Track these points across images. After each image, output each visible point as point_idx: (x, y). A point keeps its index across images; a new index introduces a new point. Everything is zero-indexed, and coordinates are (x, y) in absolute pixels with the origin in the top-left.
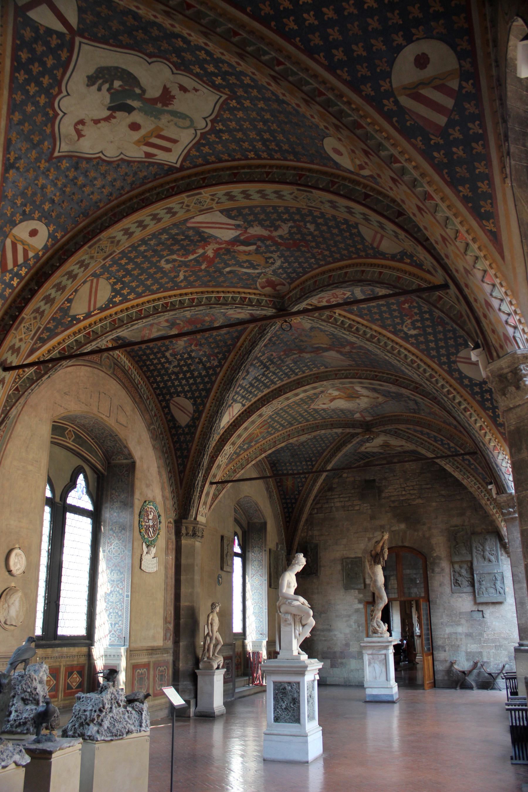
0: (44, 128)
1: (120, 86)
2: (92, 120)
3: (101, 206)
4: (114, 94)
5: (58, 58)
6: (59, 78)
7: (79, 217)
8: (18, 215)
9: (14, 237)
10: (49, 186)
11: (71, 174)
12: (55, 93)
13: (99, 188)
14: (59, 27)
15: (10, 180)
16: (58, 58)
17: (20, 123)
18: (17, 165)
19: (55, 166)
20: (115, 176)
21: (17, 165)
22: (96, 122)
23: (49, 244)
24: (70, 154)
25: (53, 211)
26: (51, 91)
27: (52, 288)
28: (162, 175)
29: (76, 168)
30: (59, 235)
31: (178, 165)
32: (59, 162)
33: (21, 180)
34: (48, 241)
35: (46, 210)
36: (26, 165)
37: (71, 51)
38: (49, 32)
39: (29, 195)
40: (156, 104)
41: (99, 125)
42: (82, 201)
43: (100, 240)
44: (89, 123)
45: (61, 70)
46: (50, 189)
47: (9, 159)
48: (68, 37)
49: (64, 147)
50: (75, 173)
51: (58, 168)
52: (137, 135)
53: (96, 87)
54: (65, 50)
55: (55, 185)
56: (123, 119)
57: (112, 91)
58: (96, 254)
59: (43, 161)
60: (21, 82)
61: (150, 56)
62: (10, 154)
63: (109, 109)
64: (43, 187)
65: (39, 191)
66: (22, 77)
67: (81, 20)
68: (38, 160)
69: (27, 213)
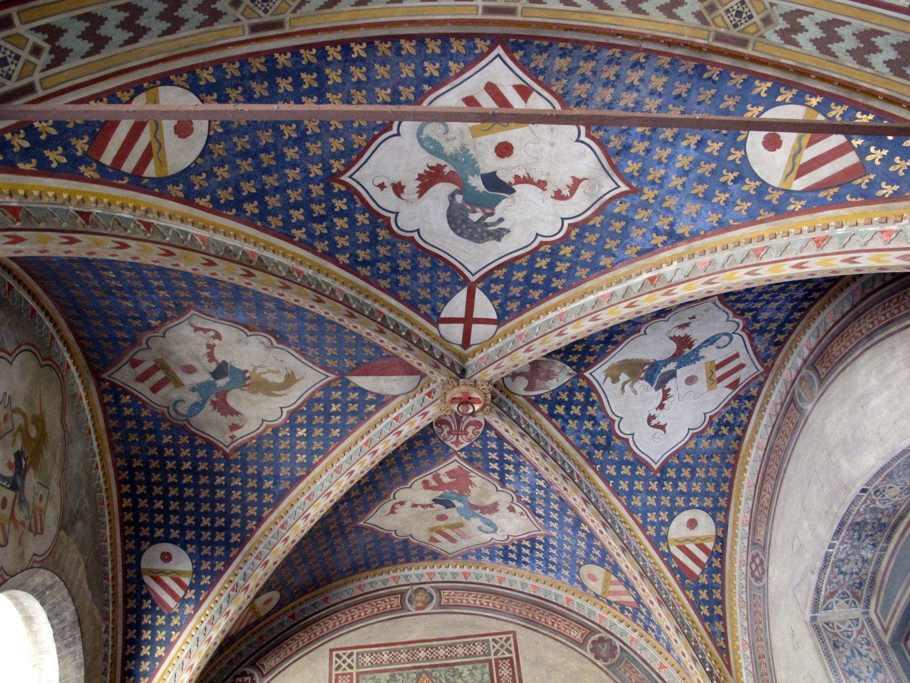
1: (474, 212)
2: (544, 189)
3: (668, 59)
4: (489, 205)
5: (509, 274)
6: (528, 257)
8: (745, 188)
9: (787, 176)
10: (678, 165)
12: (549, 246)
13: (638, 91)
14: (480, 296)
15: (692, 227)
16: (509, 274)
17: (609, 253)
18: (667, 228)
19: (641, 178)
20: (600, 90)
21: (667, 228)
22: (542, 185)
23: (789, 95)
24: (611, 172)
27: (869, 65)
28: (537, 42)
29: (627, 147)
30: (762, 88)
31: (499, 50)
32: (633, 176)
33: (685, 212)
34: (783, 103)
35: (721, 144)
36: (661, 217)
37: (491, 272)
38: (492, 297)
39: (706, 186)
40: (451, 172)
41: (543, 178)
42: (678, 97)
43: (719, 37)
44: (551, 189)
45: (517, 263)
48: (482, 284)
49: (608, 186)
50: (635, 143)
51: (643, 172)
53: (501, 226)
54: (494, 276)
55: (671, 157)
56: (506, 169)
57: (488, 211)
58: (757, 18)
59: (644, 198)
60: (564, 281)
61: (412, 239)
62: (656, 245)
63: (513, 191)
64: (683, 173)
65: (692, 176)
66: (557, 283)
67: (453, 294)
68: (645, 205)
69: (736, 174)
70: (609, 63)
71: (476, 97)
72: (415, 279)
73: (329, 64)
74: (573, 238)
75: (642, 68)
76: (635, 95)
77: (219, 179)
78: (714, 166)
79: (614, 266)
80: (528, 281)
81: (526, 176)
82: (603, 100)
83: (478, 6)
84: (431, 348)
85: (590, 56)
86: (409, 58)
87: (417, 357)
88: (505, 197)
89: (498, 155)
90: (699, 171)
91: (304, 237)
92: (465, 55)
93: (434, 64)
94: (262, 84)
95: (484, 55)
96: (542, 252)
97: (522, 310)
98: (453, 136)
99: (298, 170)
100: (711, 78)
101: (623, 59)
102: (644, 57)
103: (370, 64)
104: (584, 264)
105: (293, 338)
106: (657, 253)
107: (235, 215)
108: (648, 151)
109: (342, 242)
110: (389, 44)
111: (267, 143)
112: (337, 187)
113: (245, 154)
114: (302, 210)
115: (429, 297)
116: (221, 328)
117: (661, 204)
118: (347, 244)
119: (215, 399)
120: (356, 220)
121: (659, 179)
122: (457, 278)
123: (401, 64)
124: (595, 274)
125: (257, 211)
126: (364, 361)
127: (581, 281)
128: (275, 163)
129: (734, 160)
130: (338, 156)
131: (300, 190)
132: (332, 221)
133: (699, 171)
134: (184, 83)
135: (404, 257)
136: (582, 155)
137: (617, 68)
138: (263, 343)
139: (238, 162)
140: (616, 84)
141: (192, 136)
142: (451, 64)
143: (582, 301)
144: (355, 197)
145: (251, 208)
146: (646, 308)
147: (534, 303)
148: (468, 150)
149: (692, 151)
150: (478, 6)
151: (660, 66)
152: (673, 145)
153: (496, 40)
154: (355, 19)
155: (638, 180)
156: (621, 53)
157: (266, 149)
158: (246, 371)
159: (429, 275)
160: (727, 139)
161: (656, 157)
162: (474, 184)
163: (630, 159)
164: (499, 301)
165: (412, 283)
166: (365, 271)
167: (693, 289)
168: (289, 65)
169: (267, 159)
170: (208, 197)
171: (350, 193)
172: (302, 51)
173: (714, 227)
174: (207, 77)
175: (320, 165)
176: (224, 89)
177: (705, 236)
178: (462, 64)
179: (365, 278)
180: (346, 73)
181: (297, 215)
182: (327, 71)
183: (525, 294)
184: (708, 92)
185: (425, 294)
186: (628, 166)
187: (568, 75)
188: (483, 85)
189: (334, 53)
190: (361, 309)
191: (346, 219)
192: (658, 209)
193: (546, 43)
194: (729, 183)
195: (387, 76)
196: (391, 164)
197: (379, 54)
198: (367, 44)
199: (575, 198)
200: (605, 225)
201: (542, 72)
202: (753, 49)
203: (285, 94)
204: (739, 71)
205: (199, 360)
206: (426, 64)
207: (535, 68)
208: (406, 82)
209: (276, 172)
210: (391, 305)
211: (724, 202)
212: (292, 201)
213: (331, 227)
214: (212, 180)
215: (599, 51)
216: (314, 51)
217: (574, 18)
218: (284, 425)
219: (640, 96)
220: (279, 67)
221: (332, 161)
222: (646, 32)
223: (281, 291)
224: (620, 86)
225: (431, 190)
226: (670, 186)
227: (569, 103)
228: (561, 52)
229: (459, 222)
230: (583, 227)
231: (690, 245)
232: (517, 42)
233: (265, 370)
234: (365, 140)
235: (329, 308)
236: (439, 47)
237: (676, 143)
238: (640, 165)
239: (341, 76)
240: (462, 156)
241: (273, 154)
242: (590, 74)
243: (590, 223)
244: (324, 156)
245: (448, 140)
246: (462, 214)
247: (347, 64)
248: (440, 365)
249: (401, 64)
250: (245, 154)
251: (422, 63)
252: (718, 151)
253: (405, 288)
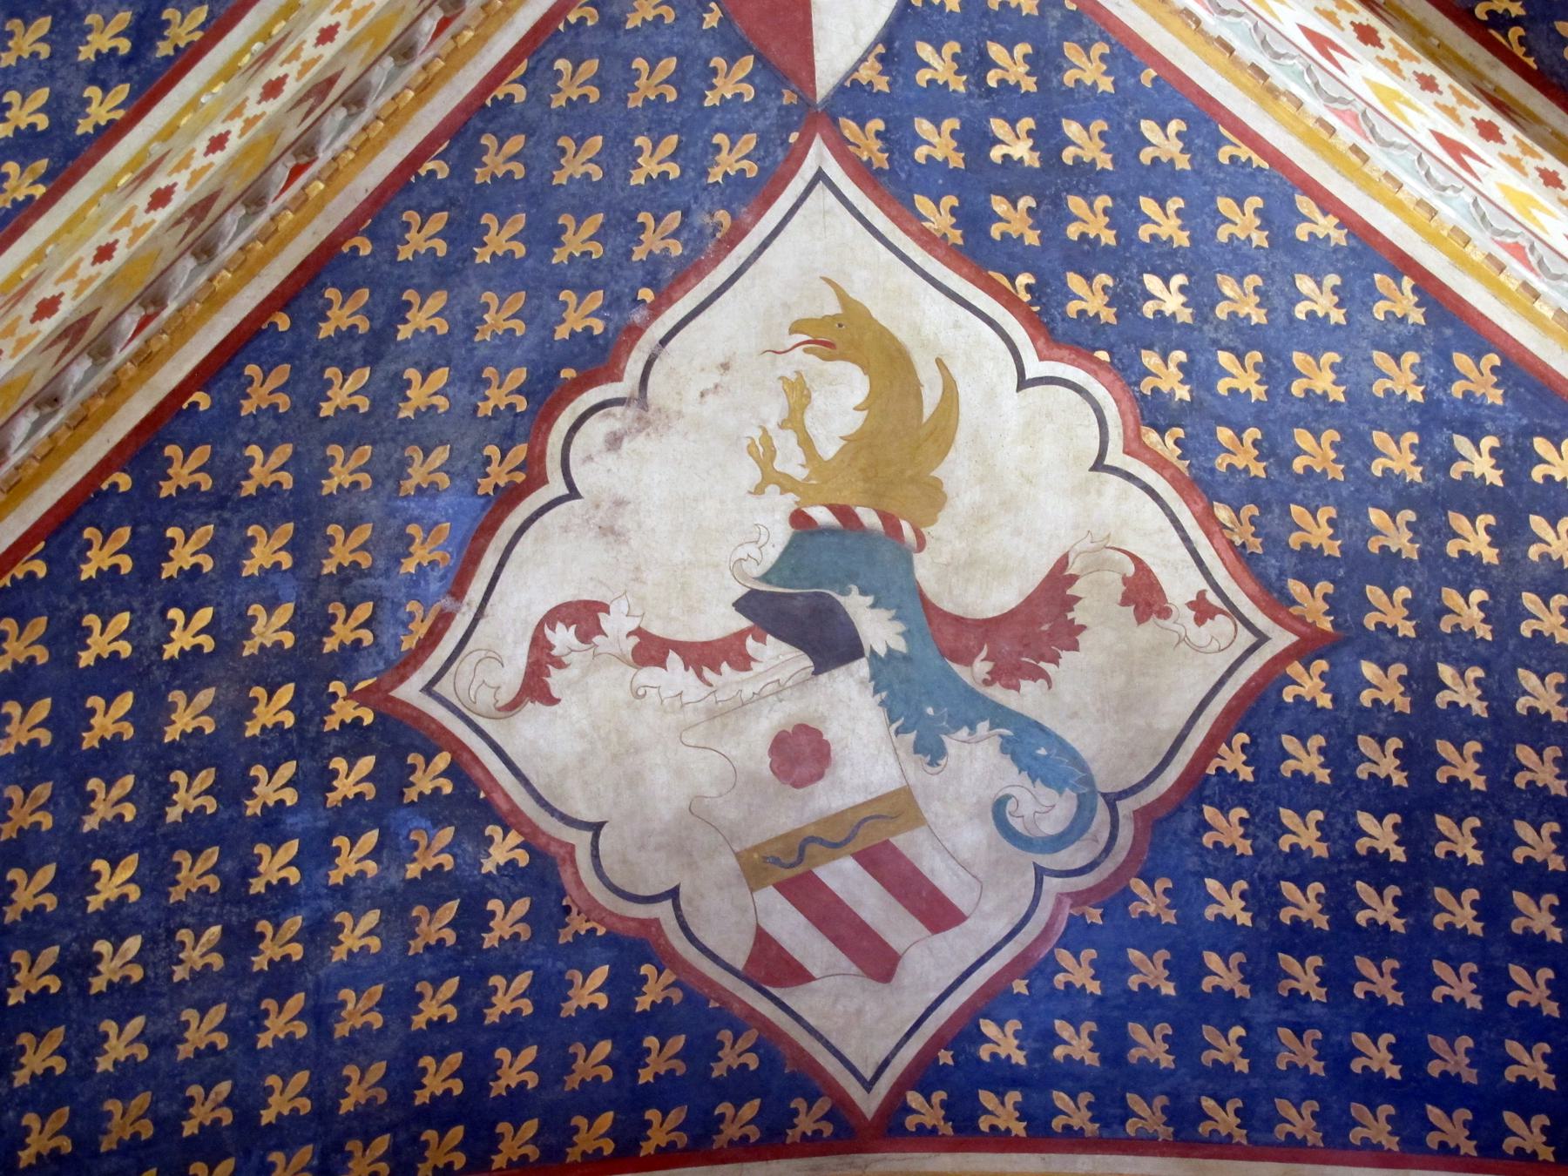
105: (580, 315)
118: (42, 95)
119: (982, 667)
138: (614, 442)
158: (799, 519)
205: (742, 706)
218: (1126, 373)
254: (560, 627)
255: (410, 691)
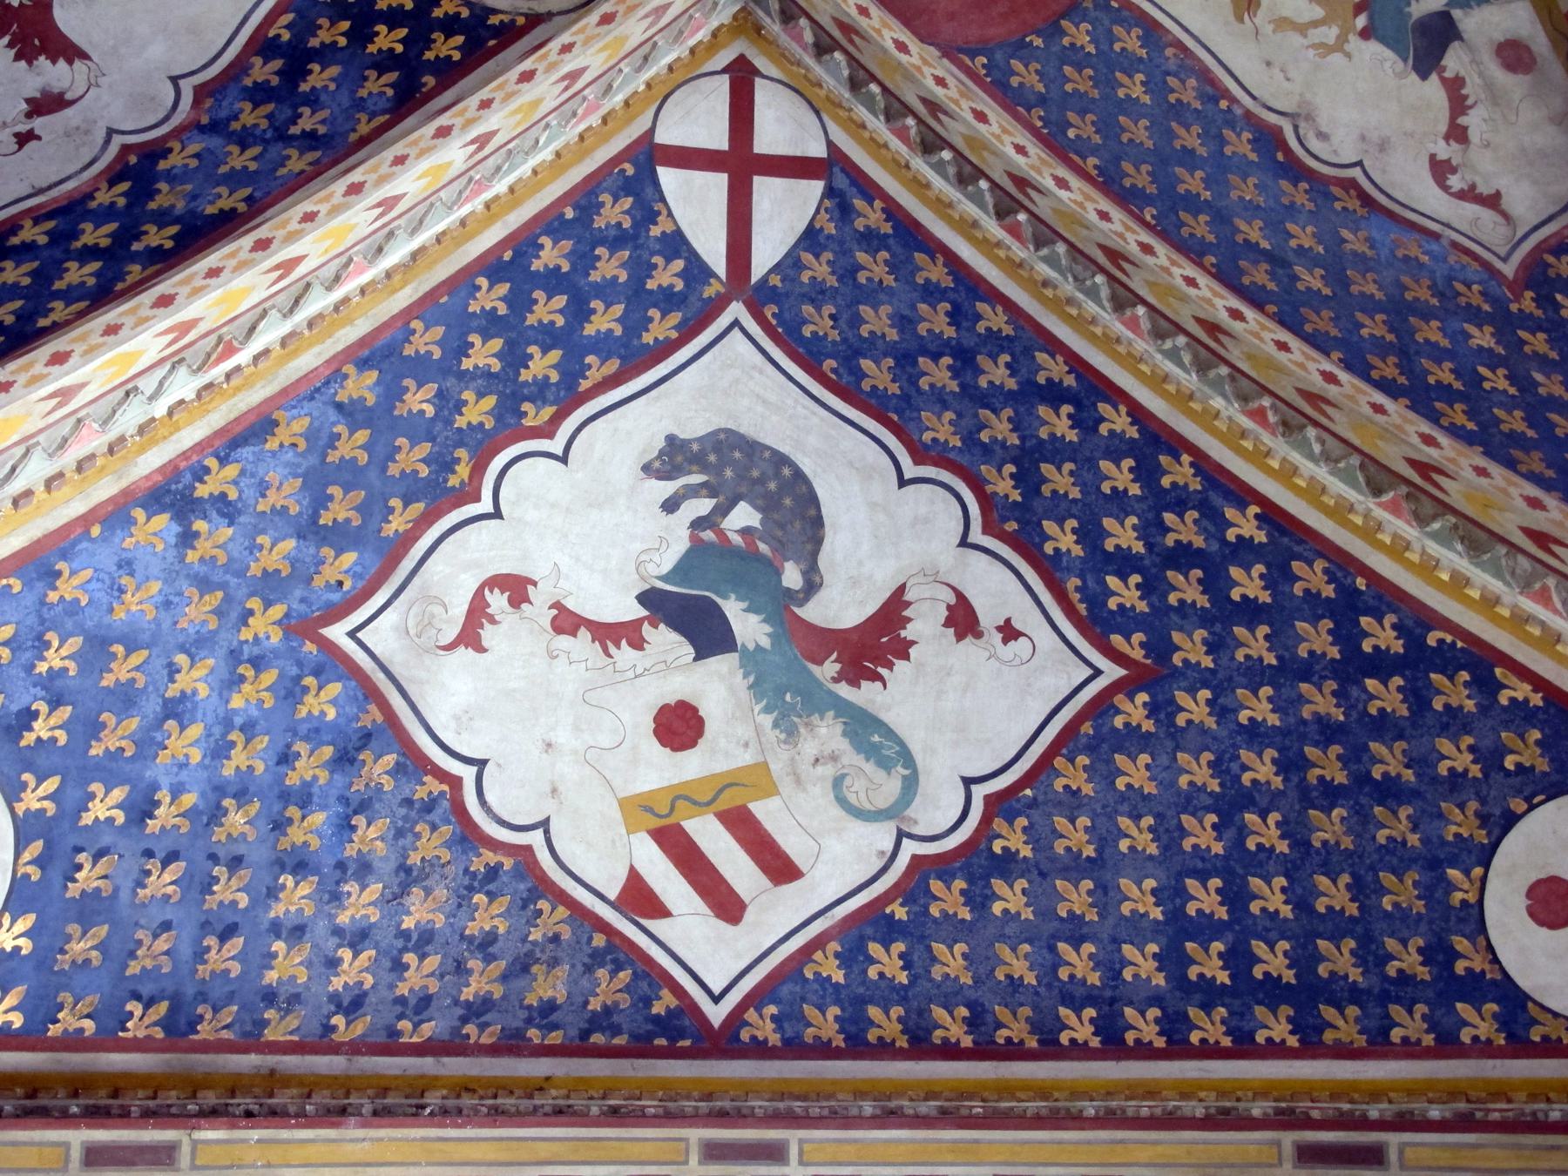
0: (395, 503)
1: (746, 532)
2: (557, 605)
3: (270, 1035)
4: (706, 553)
5: (635, 324)
6: (585, 385)
7: (149, 1004)
10: (195, 731)
11: (310, 766)
12: (528, 422)
13: (338, 931)
14: (712, 247)
15: (129, 542)
16: (635, 324)
17: (351, 412)
18: (200, 525)
19: (294, 671)
20: (440, 921)
21: (200, 525)
22: (566, 622)
24: (379, 678)
25: (98, 856)
26: (526, 407)
28: (621, 1040)
29: (345, 760)
31: (716, 1014)
32: (317, 673)
33: (155, 587)
35: (87, 819)
37: (688, 332)
38: (676, 244)
39: (108, 681)
40: (820, 663)
41: (564, 641)
42: (226, 935)
44: (539, 610)
45: (613, 366)
46: (186, 743)
47: (201, 473)
48: (710, 291)
49: (384, 634)
50: (323, 776)
51: (291, 692)
52: (664, 770)
53: (668, 488)
54: (675, 318)
55: (220, 751)
56: (668, 667)
57: (708, 535)
59: (277, 611)
60: (474, 307)
61: (920, 454)
62: (223, 461)
63: (645, 598)
64: (177, 710)
65: (152, 706)
66: (491, 298)
67: (789, 264)
68: (270, 586)
69: (29, 738)
70: (425, 1001)
71: (765, 882)
72: (904, 322)
73: (1156, 1000)
74: (462, 453)
75: (335, 998)
76: (343, 919)
77: (1469, 740)
78: (96, 750)
79: (334, 372)
80: (573, 303)
81: (612, 649)
82: (428, 892)
83: (801, 1163)
84: (855, 85)
85: (478, 1015)
86: (950, 995)
87: (909, 76)
88: (663, 578)
89: (695, 710)
90: (133, 724)
91: (1230, 513)
92: (803, 999)
93: (881, 975)
94: (1332, 973)
95: (755, 999)
96: (545, 402)
97: (585, 197)
98: (820, 769)
99: (1243, 716)
100: (147, 1006)
101: (388, 1016)
102: (334, 1028)
103: (1049, 986)
104: (421, 368)
105: (1240, 144)
106: (218, 434)
107: (1430, 629)
108: (286, 758)
109: (1120, 476)
110: (1001, 1036)
111: (1328, 811)
112: (1134, 646)
113: (1390, 792)
114: (1235, 595)
115: (862, 257)
116: (1428, 199)
117: (228, 599)
118: (1106, 466)
120: (1082, 535)
121: (242, 679)
122: (780, 309)
123: (966, 979)
124: (386, 337)
125: (1365, 621)
126: (1038, 42)
127: (423, 307)
128: (1306, 749)
129: (40, 782)
130: (1132, 740)
131: (1240, 655)
132: (1149, 546)
133: (133, 724)
134: (1541, 1016)
135: (940, 400)
136: (464, 719)
137: (403, 989)
138: (1322, 136)
139: (1409, 775)
140: (400, 943)
141: (1534, 876)
142: (839, 977)
143: (415, 244)
144: (1082, 608)
145: (1382, 636)
146: (242, 266)
147: (549, 223)
148: (776, 725)
149: (165, 782)
150: (801, 1163)
151: (288, 1012)
152: (220, 790)
153: (724, 1042)
154: (1113, 1142)
155: (300, 664)
156: (399, 1033)
157: (1330, 794)
158: (1365, 34)
159: (864, 331)
160: (74, 840)
161: (262, 742)
162: (754, 619)
163: (334, 725)
164: (655, 231)
165: (914, 307)
166: (1052, 369)
167: (110, 363)
168: (1260, 1011)
169: (1328, 766)
170: (1504, 701)
171: (1098, 623)
172: (1227, 1042)
173: (64, 556)
174: (1476, 1020)
175: (1181, 720)
176: (1436, 979)
177: (86, 520)
178: (809, 975)
179: (1054, 346)
180: (1112, 967)
181: (1248, 584)
182: (1160, 980)
183: (583, 256)
184: (149, 963)
185: (874, 267)
186: (334, 702)
187: (530, 954)
188: (749, 916)
189: (1144, 1026)
190: (1074, 260)
191: (1109, 545)
192: (234, 581)
193: (597, 1038)
194: (42, 707)
195: (1004, 951)
196: (991, 696)
197: (1026, 1011)
198: (1057, 1042)
199: (470, 584)
200: (376, 509)
201: (597, 958)
202: (66, 1146)
203: (1273, 935)
204: (74, 1042)
205: (1489, 86)
206: (903, 978)
207: (618, 967)
208: (954, 930)
209: (1304, 722)
210: (971, 239)
211: (48, 645)
212: (1263, 630)
213: (1151, 529)
214: (1487, 743)
215: (456, 1031)
216: (1195, 1038)
217: (555, 1147)
219: (332, 917)
220: (1286, 1010)
221: (1148, 726)
222: (361, 1133)
223: (1332, 391)
224: (387, 938)
225: (871, 608)
226: (211, 662)
227: (518, 874)
228: (554, 1017)
229: (788, 502)
230: (440, 495)
231: (124, 484)
232: (673, 1040)
233: (1317, 35)
234: (1058, 774)
235: (1184, 299)
236: (871, 1023)
237: (212, 797)
238: (303, 712)
239: (1125, 963)
240: (793, 706)
241: (1313, 775)
242: (471, 964)
243: (418, 507)
244: (1169, 744)
245: (834, 758)
246: (782, 526)
247: (1108, 993)
248: (837, 34)
249: (966, 979)
250: (1390, 792)
251: (914, 979)
252: (92, 796)
253: (931, 293)
254: (1449, 183)
255: (1508, 270)
